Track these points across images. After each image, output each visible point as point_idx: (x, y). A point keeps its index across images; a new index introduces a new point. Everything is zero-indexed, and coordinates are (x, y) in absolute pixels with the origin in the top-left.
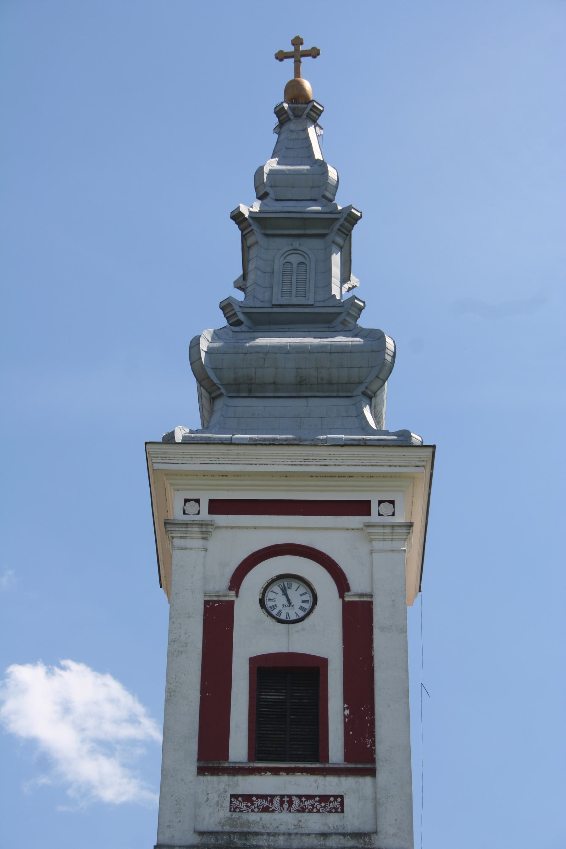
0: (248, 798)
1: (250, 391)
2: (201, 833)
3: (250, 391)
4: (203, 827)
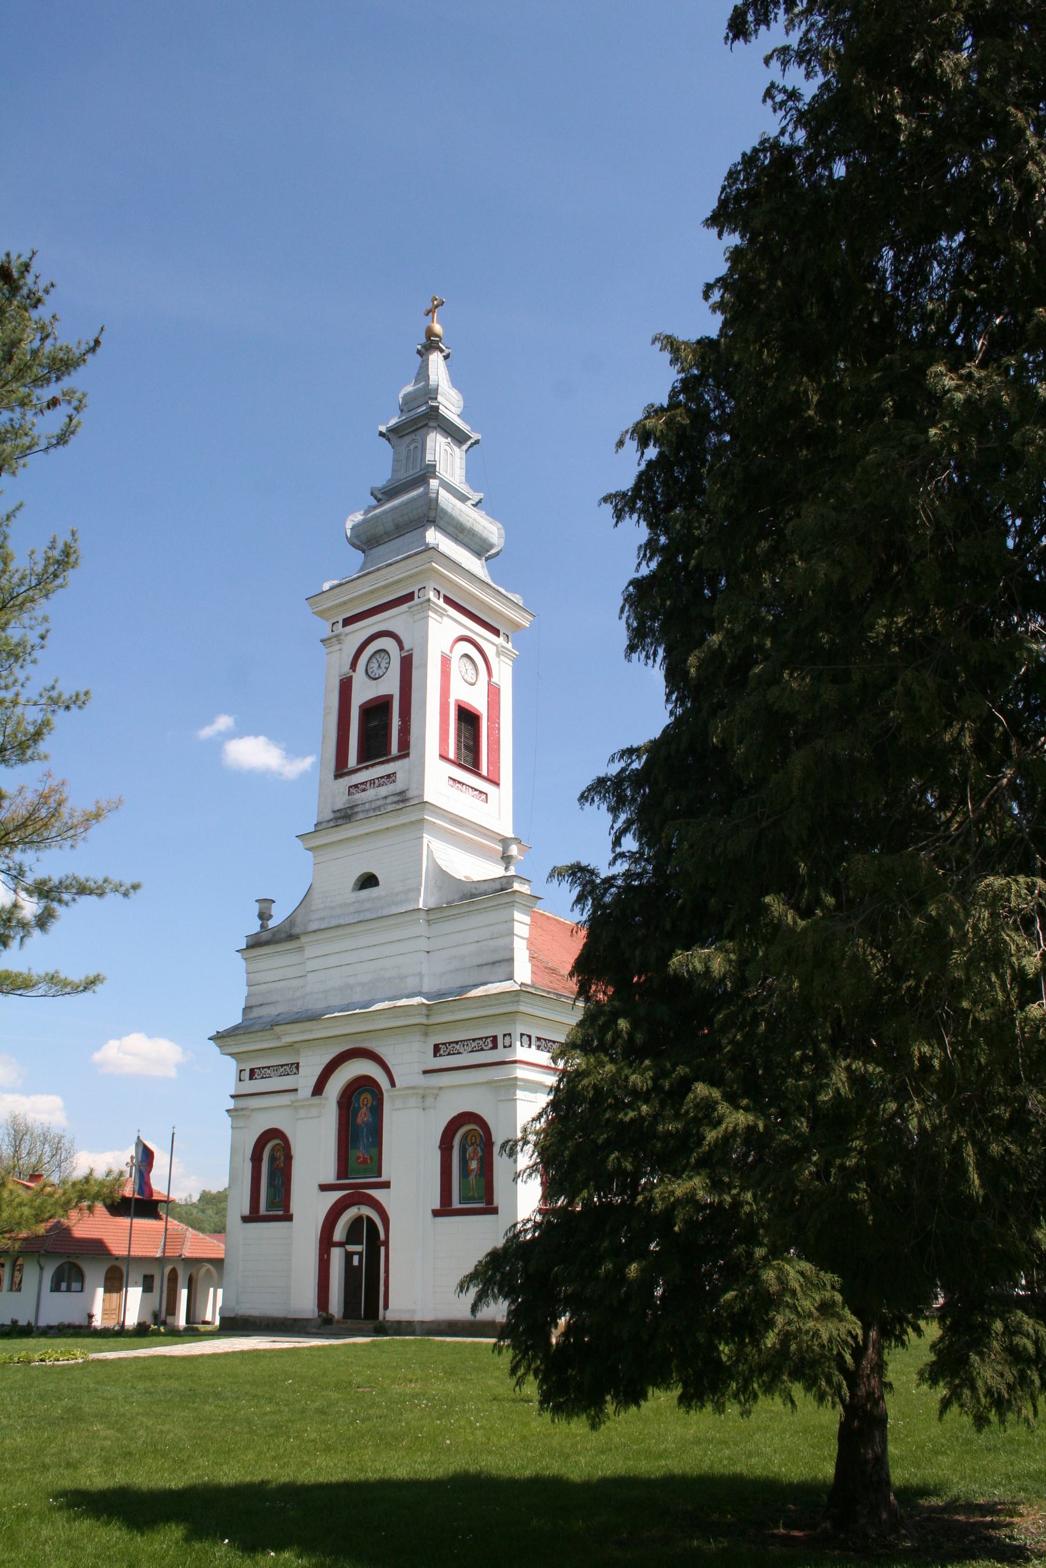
0: (356, 786)
1: (377, 542)
2: (334, 812)
3: (377, 542)
4: (336, 808)
